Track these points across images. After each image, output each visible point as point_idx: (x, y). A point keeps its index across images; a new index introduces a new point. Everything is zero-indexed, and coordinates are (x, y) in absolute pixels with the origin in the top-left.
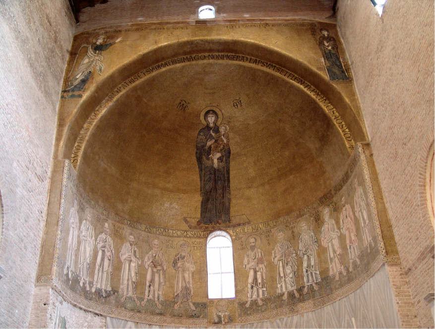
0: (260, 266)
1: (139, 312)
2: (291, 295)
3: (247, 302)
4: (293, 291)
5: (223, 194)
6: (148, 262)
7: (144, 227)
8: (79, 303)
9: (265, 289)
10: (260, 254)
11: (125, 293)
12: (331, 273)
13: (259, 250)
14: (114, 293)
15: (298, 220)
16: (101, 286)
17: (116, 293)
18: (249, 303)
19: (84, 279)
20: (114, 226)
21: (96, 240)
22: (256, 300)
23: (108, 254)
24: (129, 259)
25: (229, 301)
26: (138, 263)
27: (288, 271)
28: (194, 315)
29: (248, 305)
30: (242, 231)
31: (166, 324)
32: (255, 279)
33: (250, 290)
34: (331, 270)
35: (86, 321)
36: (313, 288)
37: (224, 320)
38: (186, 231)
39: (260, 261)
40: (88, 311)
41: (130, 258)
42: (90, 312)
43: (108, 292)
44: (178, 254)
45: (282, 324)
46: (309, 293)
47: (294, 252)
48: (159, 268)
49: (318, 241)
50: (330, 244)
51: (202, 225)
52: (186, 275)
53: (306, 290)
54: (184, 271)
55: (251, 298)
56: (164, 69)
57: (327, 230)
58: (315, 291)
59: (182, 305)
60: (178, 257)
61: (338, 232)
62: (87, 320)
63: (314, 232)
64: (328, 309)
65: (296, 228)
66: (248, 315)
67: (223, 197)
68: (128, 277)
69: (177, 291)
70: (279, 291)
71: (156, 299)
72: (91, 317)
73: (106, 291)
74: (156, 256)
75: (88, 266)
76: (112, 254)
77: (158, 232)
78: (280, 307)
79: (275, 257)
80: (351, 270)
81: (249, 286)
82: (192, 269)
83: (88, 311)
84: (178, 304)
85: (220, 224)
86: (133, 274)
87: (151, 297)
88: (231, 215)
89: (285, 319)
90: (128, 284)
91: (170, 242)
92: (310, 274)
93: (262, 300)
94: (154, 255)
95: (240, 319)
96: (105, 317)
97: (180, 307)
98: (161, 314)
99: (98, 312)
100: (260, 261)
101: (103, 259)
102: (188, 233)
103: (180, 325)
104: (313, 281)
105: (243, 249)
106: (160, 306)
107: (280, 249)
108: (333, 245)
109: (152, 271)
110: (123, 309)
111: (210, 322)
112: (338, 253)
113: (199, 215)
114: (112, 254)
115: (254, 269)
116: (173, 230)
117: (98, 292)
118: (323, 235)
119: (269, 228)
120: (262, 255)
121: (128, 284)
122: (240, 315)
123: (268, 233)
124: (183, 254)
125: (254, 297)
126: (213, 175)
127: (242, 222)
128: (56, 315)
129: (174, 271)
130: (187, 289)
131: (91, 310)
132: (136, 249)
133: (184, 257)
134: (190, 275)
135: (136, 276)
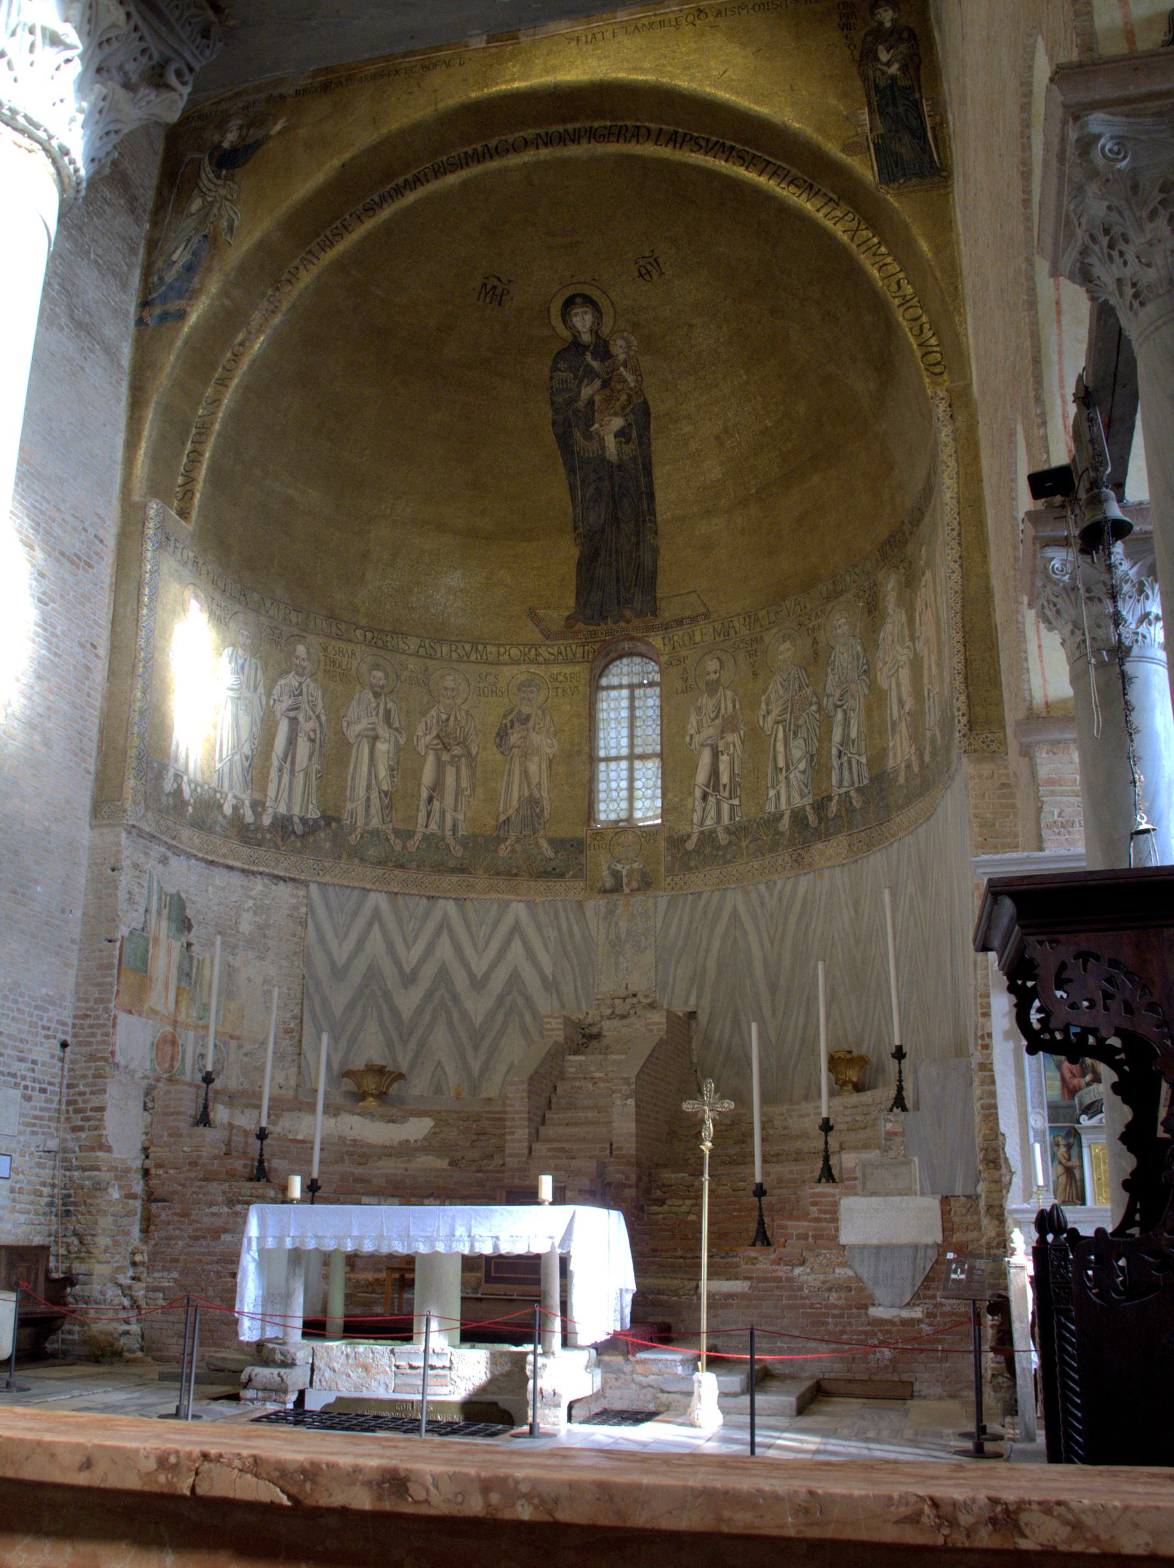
0: (730, 737)
1: (402, 866)
2: (799, 818)
3: (689, 836)
4: (803, 808)
5: (638, 533)
6: (425, 739)
7: (413, 643)
8: (225, 856)
9: (736, 802)
10: (730, 706)
11: (360, 822)
12: (891, 763)
13: (729, 693)
14: (328, 824)
15: (829, 606)
16: (289, 808)
17: (334, 825)
18: (694, 838)
19: (235, 797)
20: (325, 650)
21: (269, 694)
22: (713, 832)
23: (307, 726)
24: (371, 733)
25: (649, 833)
26: (397, 741)
27: (797, 753)
28: (549, 869)
29: (691, 845)
30: (686, 638)
31: (472, 895)
32: (715, 772)
33: (698, 804)
34: (891, 754)
35: (251, 897)
36: (851, 803)
37: (628, 884)
39: (730, 725)
40: (253, 873)
41: (374, 729)
42: (261, 873)
43: (311, 823)
44: (512, 710)
45: (771, 895)
46: (841, 816)
47: (815, 699)
48: (457, 751)
49: (868, 671)
50: (893, 680)
52: (533, 768)
53: (833, 807)
54: (525, 756)
55: (701, 825)
57: (890, 638)
58: (853, 811)
59: (518, 848)
60: (509, 718)
61: (908, 647)
62: (253, 893)
63: (863, 645)
64: (876, 862)
65: (822, 632)
66: (689, 869)
67: (638, 543)
68: (369, 780)
69: (505, 810)
70: (771, 808)
71: (449, 833)
72: (265, 886)
73: (304, 821)
74: (448, 720)
75: (247, 764)
76: (321, 724)
77: (454, 655)
78: (771, 851)
79: (769, 712)
80: (927, 758)
81: (698, 793)
82: (548, 750)
83: (253, 873)
84: (508, 843)
85: (628, 622)
86: (382, 772)
87: (433, 827)
88: (659, 595)
89: (779, 883)
90: (368, 799)
91: (491, 679)
92: (845, 765)
93: (727, 830)
94: (444, 717)
95: (669, 879)
96: (306, 884)
97: (513, 851)
98: (462, 870)
99: (282, 874)
100: (730, 725)
101: (292, 742)
102: (542, 650)
103: (514, 898)
104: (853, 783)
105: (686, 690)
106: (458, 851)
107: (781, 691)
108: (898, 685)
109: (438, 759)
110: (357, 861)
111: (592, 889)
112: (907, 708)
113: (571, 601)
114: (321, 724)
115: (712, 746)
116: (499, 645)
117: (283, 825)
118: (880, 653)
119: (758, 629)
120: (734, 706)
121: (368, 799)
122: (670, 871)
123: (755, 646)
124: (526, 710)
125: (709, 822)
126: (606, 483)
127: (688, 613)
128: (145, 891)
129: (499, 757)
130: (533, 802)
131: (261, 869)
132: (390, 705)
133: (528, 717)
134: (544, 766)
135: (392, 776)
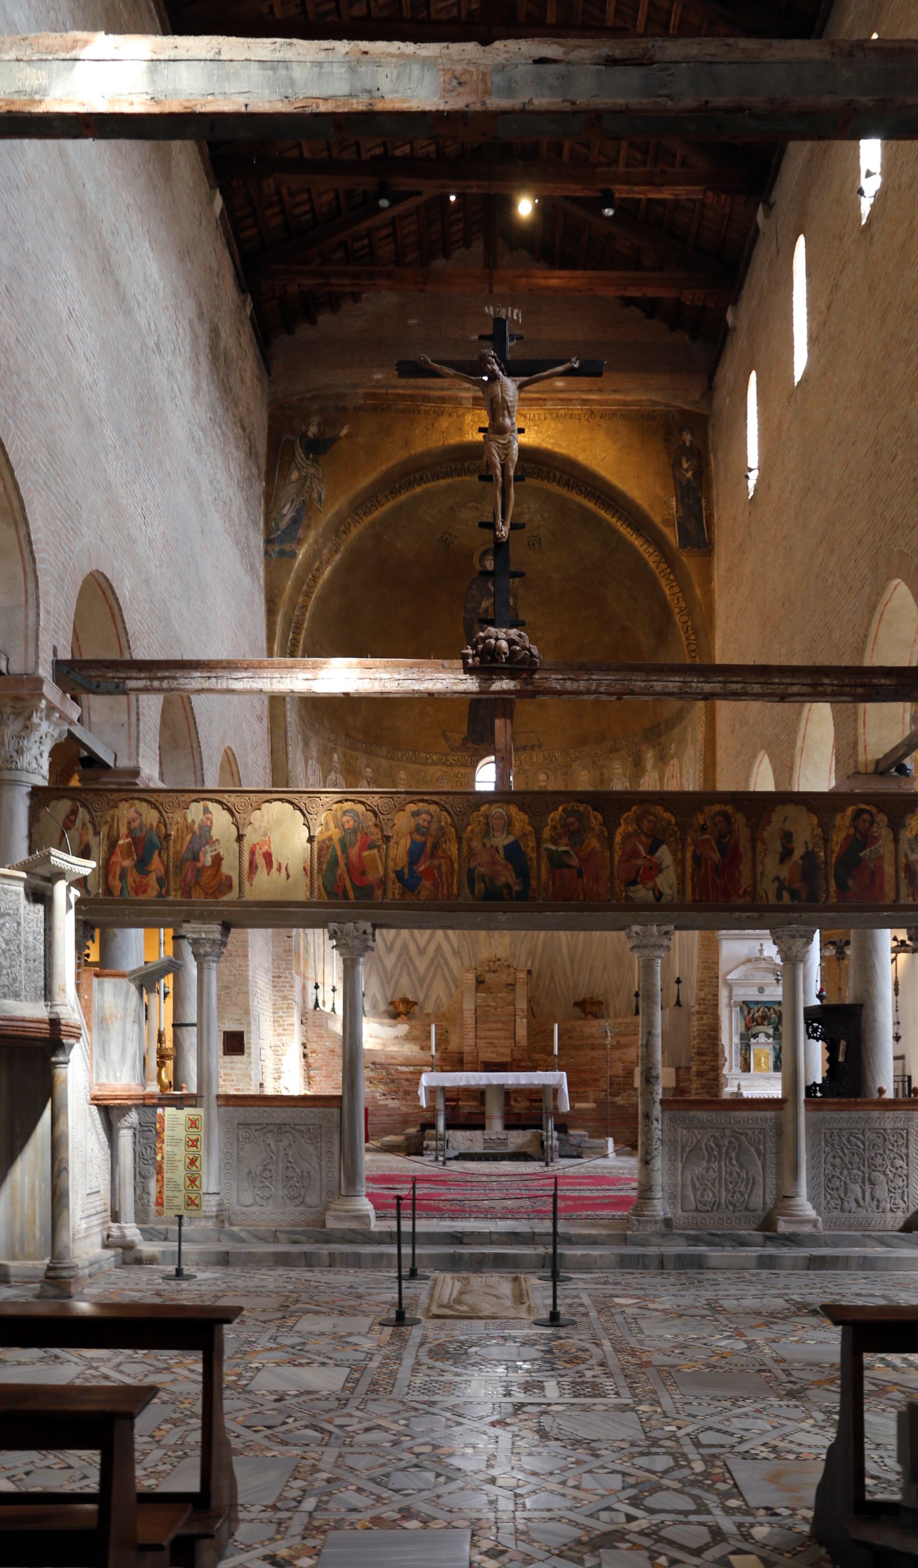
38: (446, 755)
51: (470, 744)
56: (418, 489)
113: (465, 729)
